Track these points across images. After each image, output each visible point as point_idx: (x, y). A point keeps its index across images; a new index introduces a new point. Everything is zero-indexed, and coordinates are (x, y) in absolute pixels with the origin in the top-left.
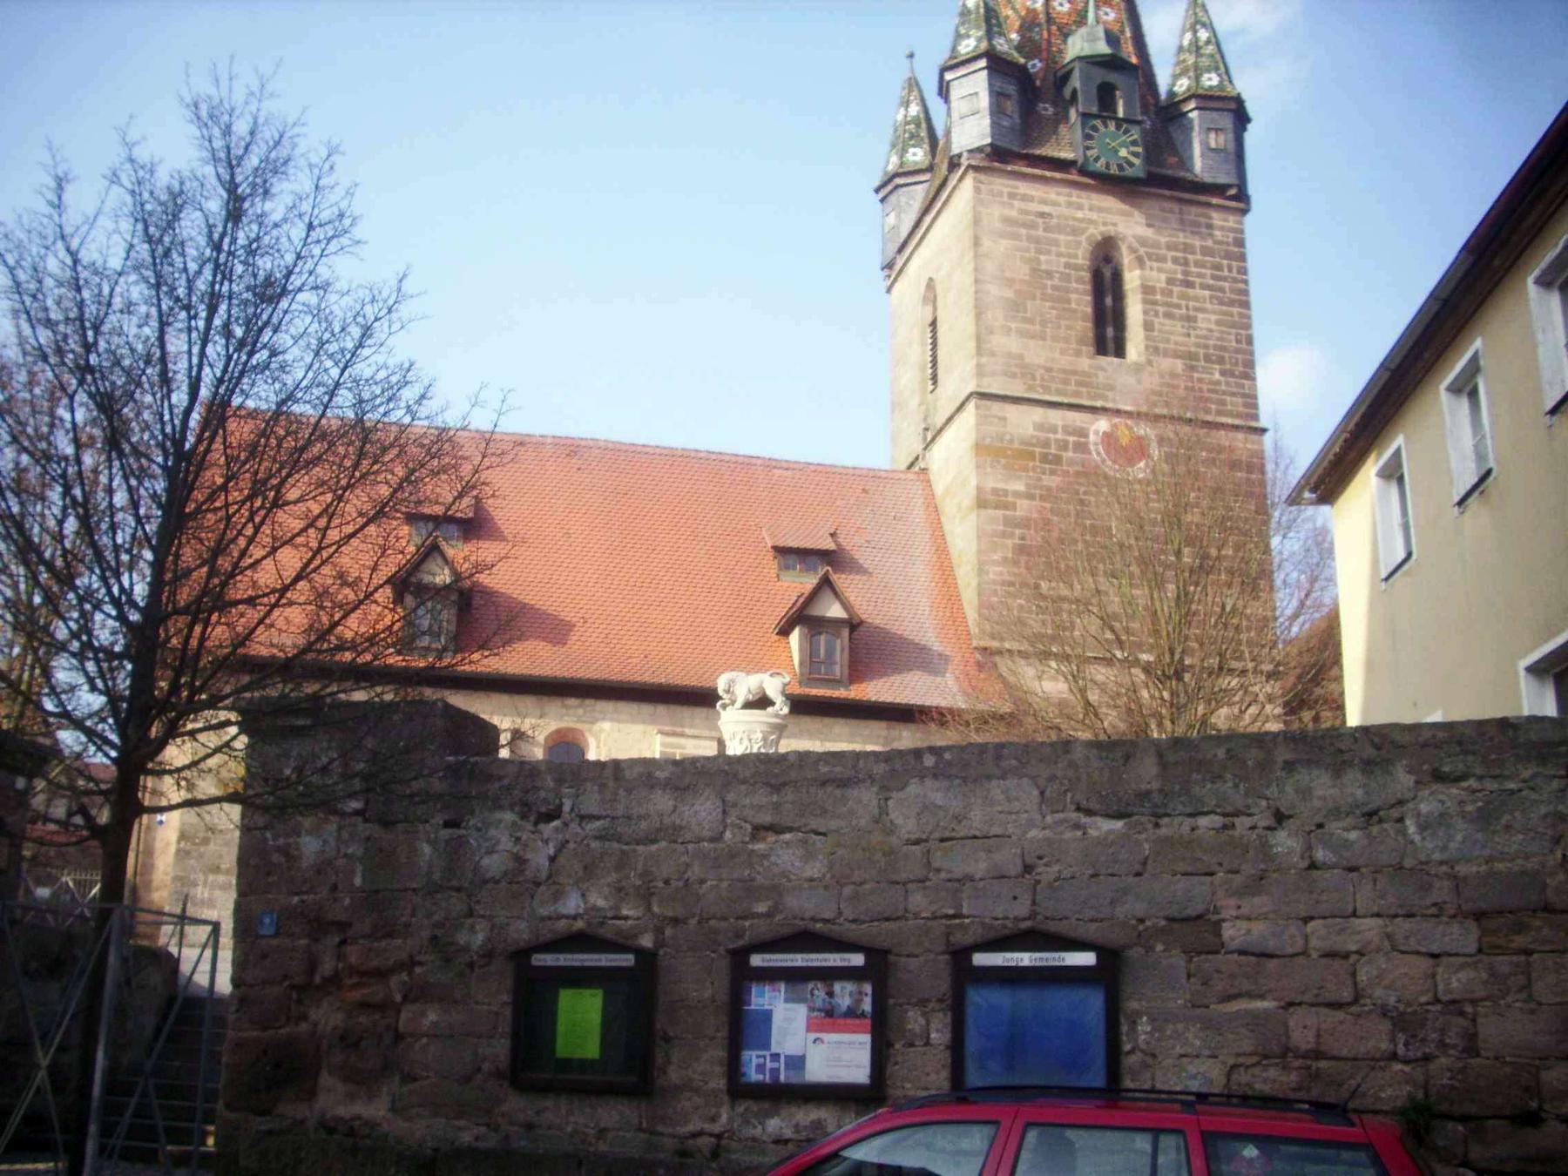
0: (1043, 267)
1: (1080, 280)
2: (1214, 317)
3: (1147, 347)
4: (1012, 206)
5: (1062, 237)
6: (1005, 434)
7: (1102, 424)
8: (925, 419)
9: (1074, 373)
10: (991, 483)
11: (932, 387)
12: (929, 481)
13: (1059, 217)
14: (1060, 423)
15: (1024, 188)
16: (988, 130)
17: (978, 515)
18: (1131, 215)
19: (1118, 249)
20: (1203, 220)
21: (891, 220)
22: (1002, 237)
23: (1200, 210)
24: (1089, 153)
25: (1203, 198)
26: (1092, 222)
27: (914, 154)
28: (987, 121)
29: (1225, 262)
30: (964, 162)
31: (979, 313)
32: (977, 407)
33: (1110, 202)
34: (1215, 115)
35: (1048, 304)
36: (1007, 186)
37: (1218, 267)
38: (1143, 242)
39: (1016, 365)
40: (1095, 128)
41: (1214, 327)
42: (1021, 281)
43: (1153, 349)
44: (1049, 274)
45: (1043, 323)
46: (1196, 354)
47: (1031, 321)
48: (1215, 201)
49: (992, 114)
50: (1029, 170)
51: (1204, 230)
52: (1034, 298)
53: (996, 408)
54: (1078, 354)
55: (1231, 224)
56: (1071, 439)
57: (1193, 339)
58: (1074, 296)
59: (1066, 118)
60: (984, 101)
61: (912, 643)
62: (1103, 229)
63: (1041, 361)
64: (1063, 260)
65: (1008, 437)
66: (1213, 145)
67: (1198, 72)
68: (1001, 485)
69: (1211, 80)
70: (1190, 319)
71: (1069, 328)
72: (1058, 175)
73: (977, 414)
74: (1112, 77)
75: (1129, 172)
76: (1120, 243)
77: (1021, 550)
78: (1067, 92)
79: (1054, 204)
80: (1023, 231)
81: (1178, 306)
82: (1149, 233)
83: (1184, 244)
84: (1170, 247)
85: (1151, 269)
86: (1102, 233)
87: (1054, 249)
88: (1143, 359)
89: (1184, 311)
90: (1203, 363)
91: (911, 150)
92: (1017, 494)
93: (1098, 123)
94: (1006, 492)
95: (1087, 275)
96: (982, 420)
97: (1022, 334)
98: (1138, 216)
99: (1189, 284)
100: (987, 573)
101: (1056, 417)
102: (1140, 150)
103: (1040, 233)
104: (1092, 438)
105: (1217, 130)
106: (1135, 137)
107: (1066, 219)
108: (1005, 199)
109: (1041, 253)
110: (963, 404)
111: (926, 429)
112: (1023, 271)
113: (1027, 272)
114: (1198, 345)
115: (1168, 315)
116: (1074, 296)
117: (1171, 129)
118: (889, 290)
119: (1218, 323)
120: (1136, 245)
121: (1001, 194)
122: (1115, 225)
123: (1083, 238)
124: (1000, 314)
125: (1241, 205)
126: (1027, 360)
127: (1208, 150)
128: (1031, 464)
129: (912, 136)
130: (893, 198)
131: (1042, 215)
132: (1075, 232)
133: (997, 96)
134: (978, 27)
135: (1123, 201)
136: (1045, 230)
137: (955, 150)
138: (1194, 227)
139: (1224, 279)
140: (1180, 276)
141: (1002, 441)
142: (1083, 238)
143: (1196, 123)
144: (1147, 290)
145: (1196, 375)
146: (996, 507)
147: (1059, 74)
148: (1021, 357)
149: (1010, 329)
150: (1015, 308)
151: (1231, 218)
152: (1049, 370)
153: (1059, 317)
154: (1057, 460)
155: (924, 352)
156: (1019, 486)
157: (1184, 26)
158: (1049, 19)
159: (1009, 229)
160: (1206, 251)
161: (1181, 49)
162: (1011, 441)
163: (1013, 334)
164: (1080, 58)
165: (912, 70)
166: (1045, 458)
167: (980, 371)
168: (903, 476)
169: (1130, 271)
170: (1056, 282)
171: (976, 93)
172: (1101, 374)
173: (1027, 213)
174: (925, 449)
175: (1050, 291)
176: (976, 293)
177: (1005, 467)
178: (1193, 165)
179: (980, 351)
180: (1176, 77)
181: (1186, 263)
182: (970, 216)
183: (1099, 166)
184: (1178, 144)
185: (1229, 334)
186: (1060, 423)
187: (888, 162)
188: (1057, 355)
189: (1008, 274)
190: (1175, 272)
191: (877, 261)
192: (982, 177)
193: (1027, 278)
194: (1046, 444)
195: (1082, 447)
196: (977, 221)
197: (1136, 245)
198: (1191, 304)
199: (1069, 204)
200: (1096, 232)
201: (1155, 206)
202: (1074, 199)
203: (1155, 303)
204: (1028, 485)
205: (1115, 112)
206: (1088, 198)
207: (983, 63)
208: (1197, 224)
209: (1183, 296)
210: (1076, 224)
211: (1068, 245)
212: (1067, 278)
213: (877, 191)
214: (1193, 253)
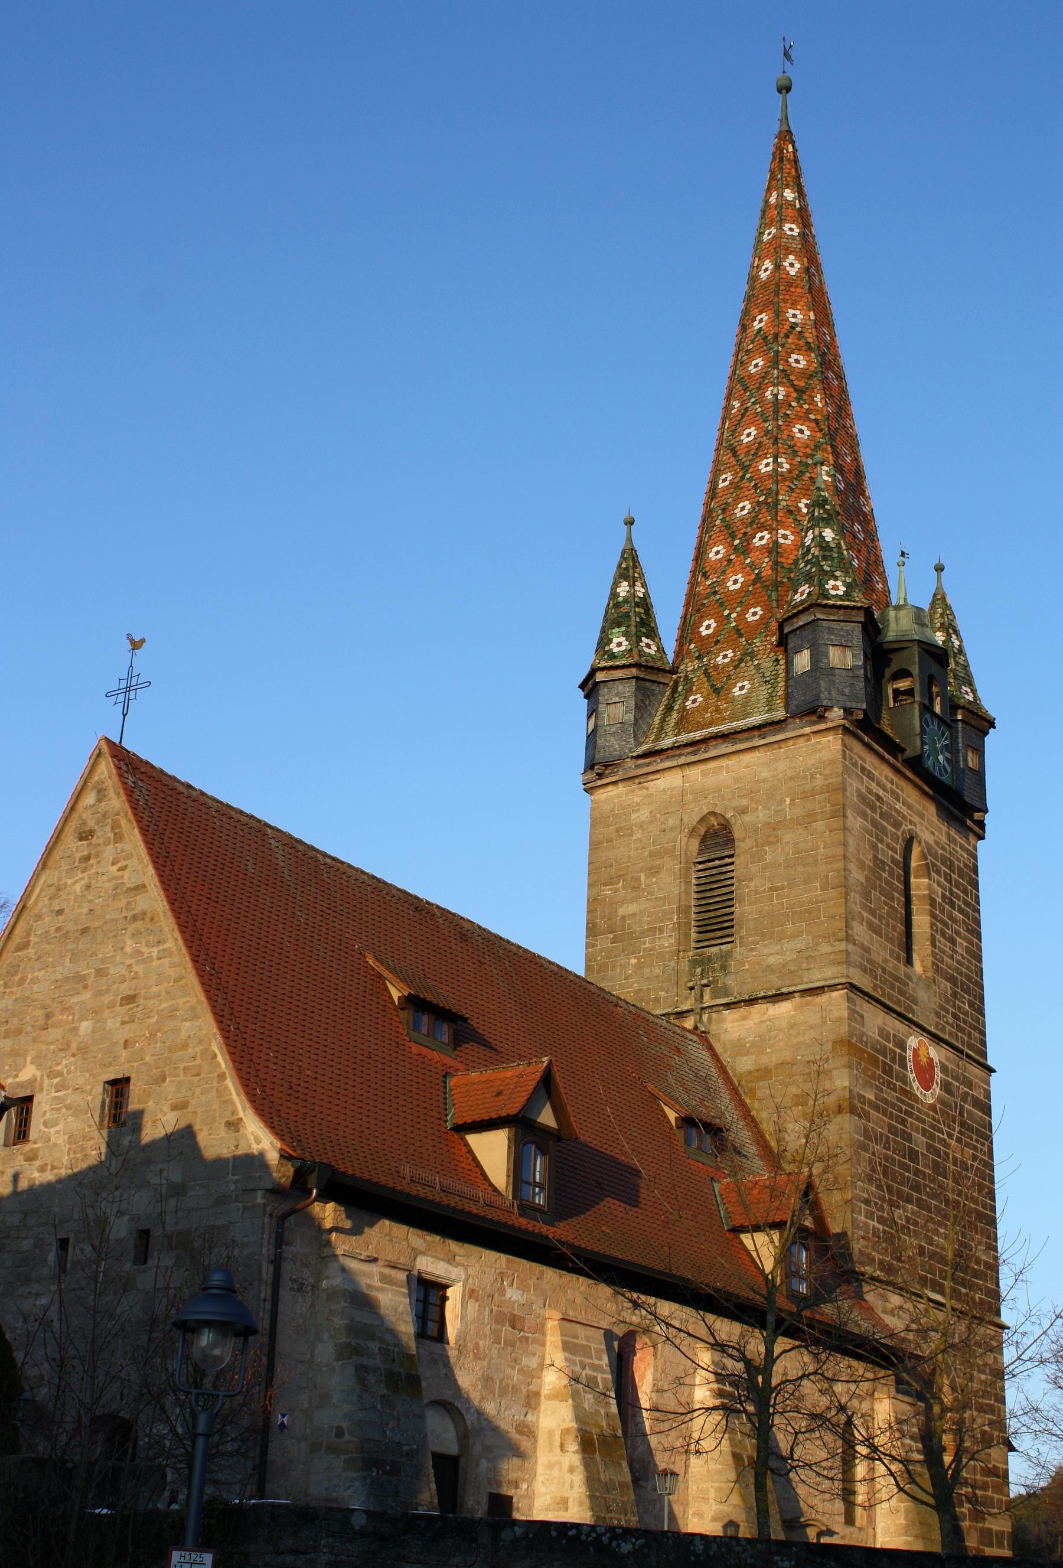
2: (965, 944)
3: (933, 963)
9: (897, 978)
10: (857, 1090)
15: (870, 762)
35: (883, 898)
54: (898, 958)
56: (898, 1051)
62: (910, 827)
73: (849, 1008)
74: (934, 668)
86: (909, 830)
89: (950, 932)
96: (855, 1016)
97: (871, 926)
108: (859, 772)
132: (897, 825)
141: (861, 1041)
148: (867, 950)
165: (629, 540)
169: (916, 877)
172: (910, 983)
177: (864, 1071)
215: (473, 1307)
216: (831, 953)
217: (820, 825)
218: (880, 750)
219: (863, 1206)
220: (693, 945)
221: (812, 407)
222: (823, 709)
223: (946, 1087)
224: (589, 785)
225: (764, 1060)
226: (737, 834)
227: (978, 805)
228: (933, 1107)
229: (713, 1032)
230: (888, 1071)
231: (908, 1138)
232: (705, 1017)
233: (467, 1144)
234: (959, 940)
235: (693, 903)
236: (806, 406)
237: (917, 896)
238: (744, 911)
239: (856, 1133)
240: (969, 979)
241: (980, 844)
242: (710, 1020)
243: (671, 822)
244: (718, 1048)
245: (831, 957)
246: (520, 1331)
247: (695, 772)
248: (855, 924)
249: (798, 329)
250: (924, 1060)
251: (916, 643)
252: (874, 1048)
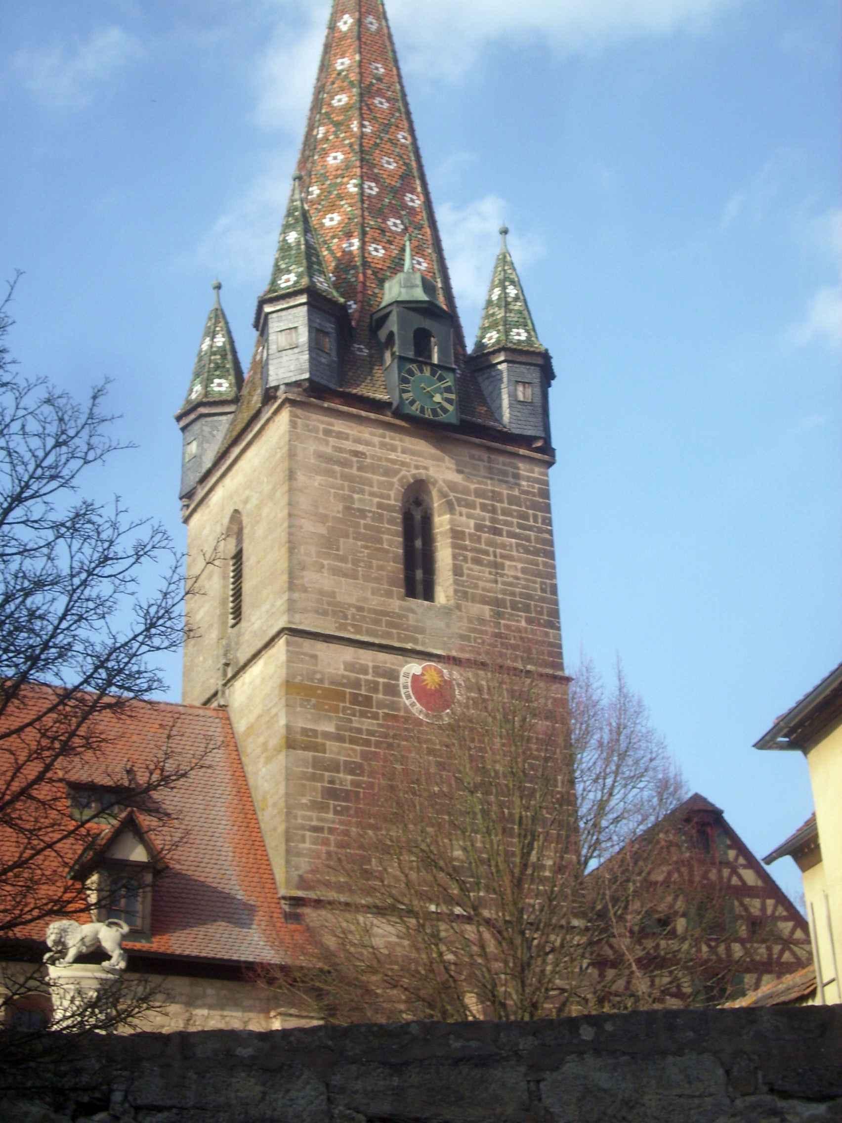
0: (356, 506)
1: (391, 521)
2: (520, 565)
3: (456, 591)
4: (327, 443)
5: (376, 477)
6: (315, 672)
7: (415, 667)
8: (225, 655)
10: (301, 724)
11: (233, 621)
12: (228, 719)
13: (373, 457)
14: (371, 664)
15: (339, 425)
16: (306, 366)
17: (287, 756)
18: (442, 460)
19: (429, 493)
20: (510, 470)
21: (193, 448)
22: (317, 473)
23: (508, 460)
24: (405, 396)
25: (509, 448)
26: (403, 464)
27: (220, 385)
28: (306, 357)
29: (531, 512)
30: (281, 394)
31: (292, 548)
32: (288, 643)
33: (421, 446)
34: (523, 369)
35: (359, 543)
36: (322, 422)
37: (524, 516)
38: (453, 487)
39: (329, 604)
40: (411, 373)
41: (520, 575)
42: (334, 518)
43: (462, 594)
44: (362, 513)
45: (356, 562)
46: (504, 601)
47: (343, 559)
48: (522, 452)
49: (311, 350)
50: (345, 408)
51: (511, 479)
52: (347, 536)
53: (307, 645)
54: (389, 594)
55: (536, 475)
57: (500, 585)
58: (385, 537)
59: (381, 361)
60: (303, 336)
61: (215, 890)
62: (414, 471)
63: (353, 600)
64: (376, 500)
65: (318, 676)
66: (521, 397)
67: (508, 326)
68: (310, 726)
69: (519, 335)
70: (496, 565)
71: (381, 568)
72: (372, 416)
73: (288, 651)
74: (427, 324)
75: (443, 417)
76: (431, 487)
77: (332, 793)
78: (383, 335)
79: (367, 443)
80: (337, 468)
81: (486, 553)
82: (458, 478)
83: (493, 492)
84: (479, 494)
85: (461, 515)
86: (414, 476)
87: (367, 488)
88: (452, 602)
90: (509, 610)
91: (217, 381)
92: (326, 735)
93: (414, 367)
94: (315, 732)
95: (398, 516)
96: (293, 657)
97: (336, 572)
98: (449, 462)
99: (496, 532)
100: (295, 817)
101: (367, 657)
102: (453, 396)
103: (354, 471)
104: (402, 680)
105: (524, 383)
106: (449, 384)
107: (380, 459)
108: (321, 435)
109: (353, 492)
111: (227, 665)
112: (336, 509)
113: (340, 508)
114: (504, 592)
115: (477, 561)
116: (385, 537)
117: (480, 379)
118: (186, 520)
119: (524, 571)
120: (446, 489)
121: (316, 430)
122: (426, 468)
123: (395, 480)
124: (313, 550)
125: (546, 458)
126: (339, 598)
127: (515, 401)
128: (342, 705)
129: (217, 367)
130: (196, 427)
131: (356, 454)
132: (387, 473)
133: (316, 332)
134: (298, 263)
135: (438, 449)
136: (360, 469)
137: (272, 384)
138: (502, 477)
139: (530, 528)
140: (488, 523)
142: (395, 480)
143: (505, 375)
144: (456, 534)
145: (502, 622)
146: (305, 748)
147: (376, 316)
148: (333, 594)
149: (323, 566)
150: (329, 543)
151: (537, 469)
152: (360, 609)
153: (370, 556)
154: (368, 701)
155: (225, 587)
156: (330, 728)
157: (493, 281)
158: (365, 264)
159: (324, 465)
160: (512, 500)
161: (489, 303)
162: (321, 681)
163: (325, 571)
164: (398, 303)
166: (355, 699)
167: (291, 607)
168: (201, 712)
169: (439, 516)
170: (369, 521)
171: (295, 328)
172: (411, 615)
173: (340, 450)
174: (225, 685)
175: (363, 531)
176: (290, 527)
177: (314, 707)
178: (501, 416)
179: (292, 586)
180: (485, 330)
181: (494, 511)
182: (285, 450)
183: (415, 409)
184: (486, 393)
185: (535, 582)
186: (371, 664)
187: (191, 390)
188: (369, 594)
189: (321, 510)
190: (484, 519)
191: (176, 489)
192: (299, 412)
193: (340, 515)
194: (357, 684)
195: (392, 690)
196: (292, 454)
197: (446, 489)
198: (498, 551)
199: (383, 445)
200: (409, 474)
201: (465, 453)
202: (387, 440)
203: (465, 548)
204: (338, 728)
205: (430, 357)
206: (401, 440)
207: (303, 299)
208: (505, 473)
209: (490, 543)
210: (389, 464)
211: (381, 484)
212: (379, 518)
213: (179, 418)
214: (501, 501)
217: (278, 494)
218: (354, 411)
219: (308, 833)
221: (348, 134)
222: (272, 390)
232: (227, 692)
234: (507, 563)
236: (342, 135)
237: (441, 533)
239: (297, 766)
240: (529, 597)
241: (552, 471)
247: (227, 481)
249: (344, 73)
251: (395, 305)
252: (332, 683)
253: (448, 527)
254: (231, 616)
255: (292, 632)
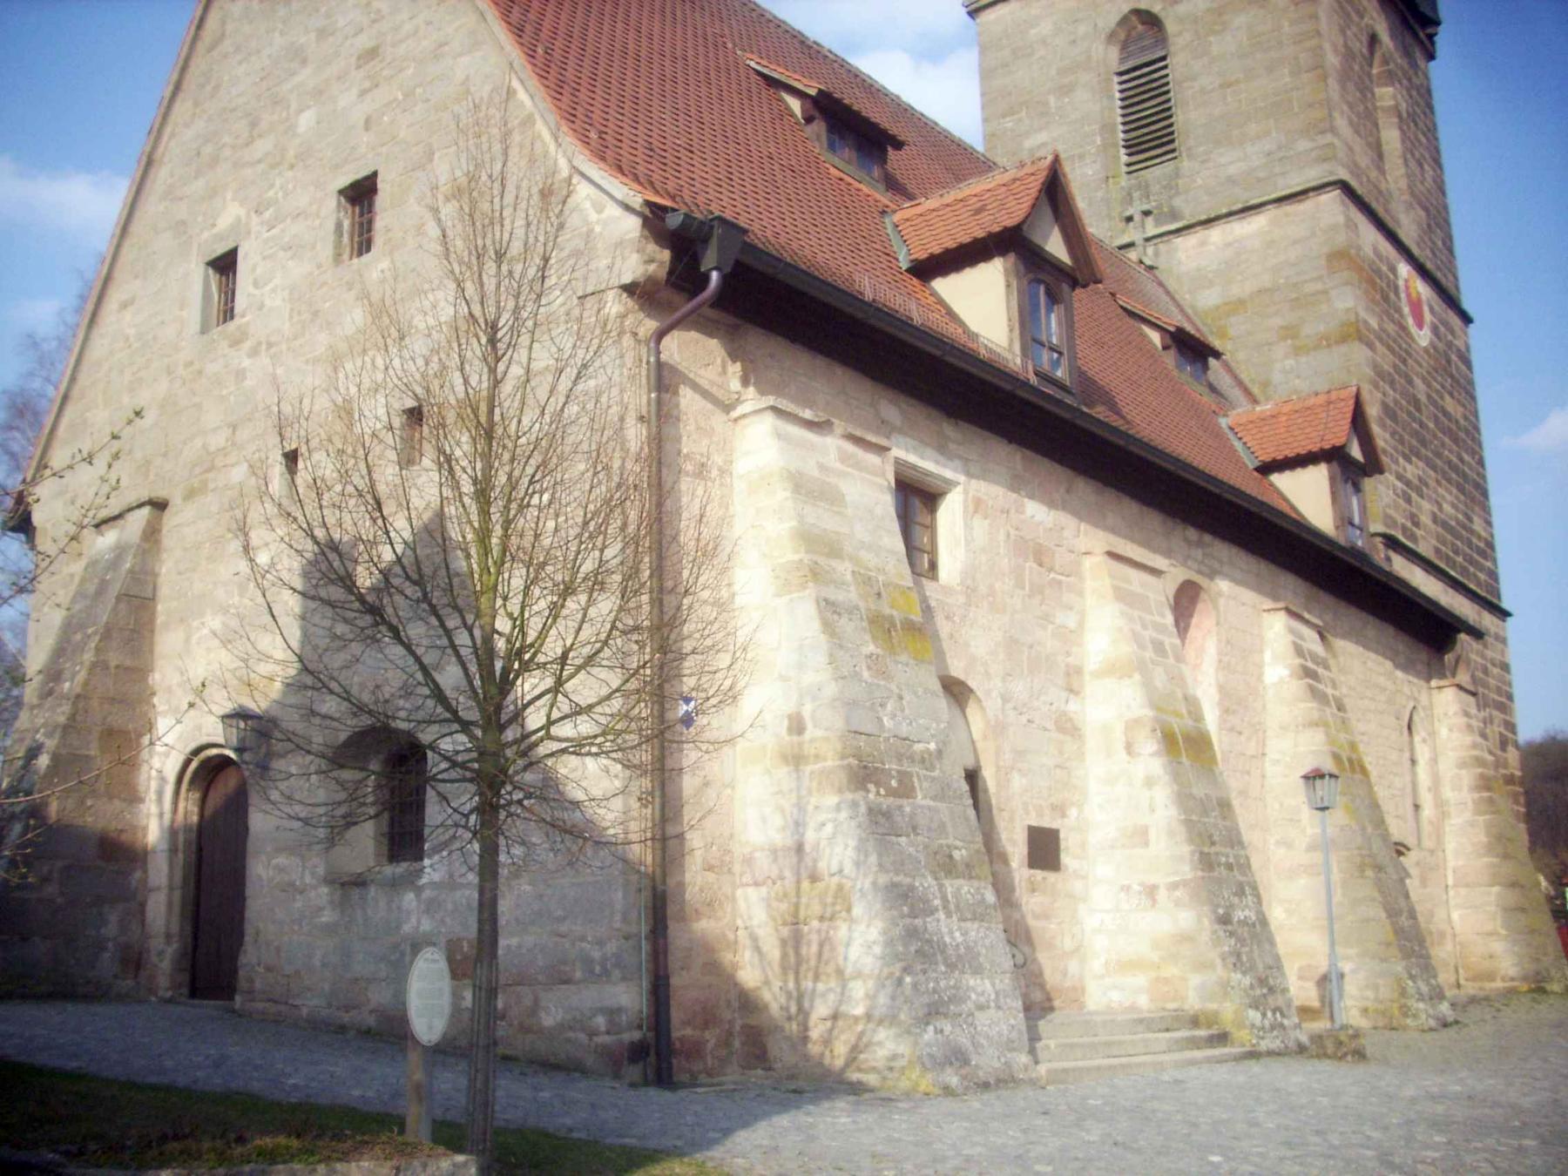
10: (1363, 314)
97: (1351, 123)
110: (1304, 192)
215: (980, 526)
216: (1312, 150)
220: (1125, 169)
223: (1435, 330)
224: (973, 7)
225: (1236, 291)
226: (1171, 27)
227: (1430, 14)
228: (1426, 350)
229: (1161, 267)
230: (1386, 298)
231: (1410, 382)
232: (1150, 250)
233: (934, 294)
235: (1120, 120)
238: (1188, 117)
241: (1432, 64)
242: (1157, 254)
243: (1082, 29)
244: (1171, 284)
245: (1314, 154)
246: (1051, 570)
248: (1336, 114)
250: (1414, 295)
253: (1392, 103)
254: (1123, 151)
255: (1345, 188)
